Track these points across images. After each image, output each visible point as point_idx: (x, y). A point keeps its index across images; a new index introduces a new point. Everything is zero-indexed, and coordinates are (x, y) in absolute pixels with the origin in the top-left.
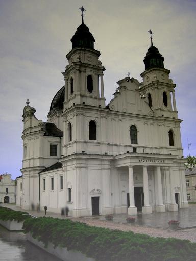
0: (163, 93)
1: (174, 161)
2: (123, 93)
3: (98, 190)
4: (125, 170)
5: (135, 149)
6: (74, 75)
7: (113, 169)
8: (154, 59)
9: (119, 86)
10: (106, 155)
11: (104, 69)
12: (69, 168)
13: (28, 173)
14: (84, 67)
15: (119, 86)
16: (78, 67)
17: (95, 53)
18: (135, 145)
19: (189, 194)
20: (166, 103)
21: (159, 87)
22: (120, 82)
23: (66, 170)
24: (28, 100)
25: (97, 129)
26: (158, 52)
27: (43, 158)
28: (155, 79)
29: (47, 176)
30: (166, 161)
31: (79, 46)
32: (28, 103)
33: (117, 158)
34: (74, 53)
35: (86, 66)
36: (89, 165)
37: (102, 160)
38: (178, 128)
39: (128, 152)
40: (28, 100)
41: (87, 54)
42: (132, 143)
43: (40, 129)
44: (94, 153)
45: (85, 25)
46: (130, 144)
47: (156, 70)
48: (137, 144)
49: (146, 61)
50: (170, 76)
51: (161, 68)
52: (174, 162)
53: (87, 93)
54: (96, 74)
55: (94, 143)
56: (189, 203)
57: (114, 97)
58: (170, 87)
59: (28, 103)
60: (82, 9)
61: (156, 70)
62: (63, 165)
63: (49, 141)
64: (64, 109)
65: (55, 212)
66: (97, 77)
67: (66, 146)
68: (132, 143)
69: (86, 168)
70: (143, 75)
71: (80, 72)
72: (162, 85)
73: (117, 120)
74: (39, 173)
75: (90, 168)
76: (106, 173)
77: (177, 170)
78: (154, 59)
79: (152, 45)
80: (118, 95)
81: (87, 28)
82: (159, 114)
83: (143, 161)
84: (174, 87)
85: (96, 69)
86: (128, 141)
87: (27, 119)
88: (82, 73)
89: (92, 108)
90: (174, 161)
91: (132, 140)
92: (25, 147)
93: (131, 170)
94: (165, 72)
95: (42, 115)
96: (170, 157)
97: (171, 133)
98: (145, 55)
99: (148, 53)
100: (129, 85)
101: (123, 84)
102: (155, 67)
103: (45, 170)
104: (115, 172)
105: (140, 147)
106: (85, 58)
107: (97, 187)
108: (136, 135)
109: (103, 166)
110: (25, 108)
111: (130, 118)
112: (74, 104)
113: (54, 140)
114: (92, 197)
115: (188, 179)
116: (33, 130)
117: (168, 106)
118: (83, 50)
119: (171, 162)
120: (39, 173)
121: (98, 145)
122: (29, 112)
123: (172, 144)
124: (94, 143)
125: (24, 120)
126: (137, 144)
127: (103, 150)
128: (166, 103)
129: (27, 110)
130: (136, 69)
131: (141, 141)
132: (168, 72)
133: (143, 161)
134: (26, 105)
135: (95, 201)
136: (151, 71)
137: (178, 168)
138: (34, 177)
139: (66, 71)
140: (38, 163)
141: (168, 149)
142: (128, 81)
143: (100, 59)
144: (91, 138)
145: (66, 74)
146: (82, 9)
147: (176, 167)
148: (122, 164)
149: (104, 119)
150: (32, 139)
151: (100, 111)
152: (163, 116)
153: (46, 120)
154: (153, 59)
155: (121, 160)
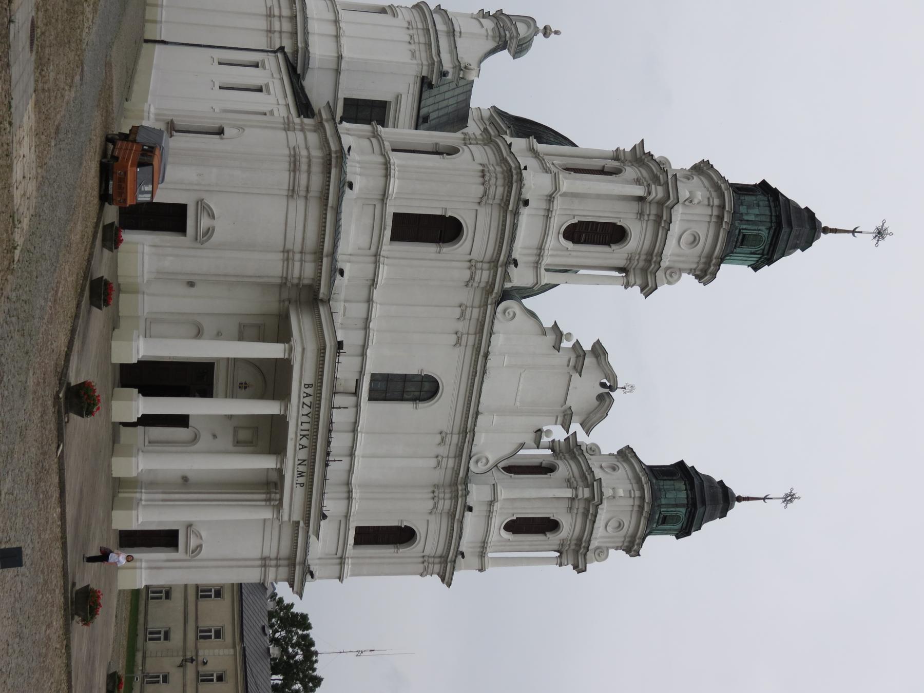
0: (555, 518)
1: (302, 524)
2: (561, 359)
3: (209, 232)
4: (282, 334)
6: (625, 186)
7: (285, 295)
8: (686, 499)
9: (587, 347)
11: (647, 290)
12: (297, 138)
13: (286, 12)
14: (659, 217)
15: (587, 347)
16: (658, 192)
17: (708, 263)
19: (167, 637)
20: (517, 526)
21: (580, 506)
22: (599, 351)
23: (288, 127)
24: (557, 33)
26: (712, 518)
27: (338, 71)
28: (608, 492)
29: (272, 74)
30: (299, 493)
31: (737, 203)
32: (547, 32)
33: (323, 310)
34: (718, 188)
35: (662, 222)
36: (301, 203)
37: (319, 254)
39: (340, 345)
40: (557, 33)
41: (705, 233)
42: (373, 375)
43: (447, 66)
44: (343, 222)
46: (370, 369)
47: (642, 498)
48: (371, 398)
49: (681, 472)
50: (618, 557)
51: (649, 520)
52: (298, 523)
53: (561, 220)
54: (630, 259)
55: (382, 228)
56: (136, 593)
57: (548, 324)
58: (576, 552)
59: (547, 32)
60: (880, 233)
61: (642, 498)
62: (307, 121)
63: (398, 98)
64: (509, 139)
65: (136, 87)
66: (622, 263)
67: (376, 135)
68: (373, 375)
69: (292, 192)
70: (627, 454)
71: (641, 199)
73: (461, 326)
74: (282, 49)
75: (292, 204)
76: (271, 266)
77: (266, 553)
78: (686, 499)
79: (740, 499)
80: (551, 338)
81: (806, 244)
82: (477, 494)
83: (307, 401)
84: (576, 567)
85: (649, 261)
86: (381, 360)
87: (489, 24)
88: (635, 206)
89: (506, 234)
90: (302, 524)
91: (388, 379)
92: (383, 11)
93: (273, 350)
94: (634, 537)
95: (499, 85)
96: (312, 515)
97: (401, 536)
98: (701, 470)
99: (709, 479)
100: (585, 388)
101: (589, 361)
102: (655, 497)
103: (295, 70)
104: (271, 304)
105: (357, 406)
106: (692, 223)
107: (223, 229)
108: (402, 399)
109: (298, 256)
110: (529, 21)
113: (406, 110)
114: (183, 208)
115: (227, 595)
116: (444, 43)
117: (506, 535)
118: (720, 218)
119: (296, 516)
120: (282, 49)
121: (373, 248)
122: (510, 35)
123: (368, 536)
124: (382, 228)
125: (484, 15)
126: (371, 398)
128: (517, 526)
129: (522, 29)
130: (649, 427)
133: (307, 401)
134: (541, 27)
135: (171, 219)
136: (639, 481)
137: (273, 555)
138: (270, 31)
139: (650, 155)
140: (320, 49)
141: (347, 516)
142: (603, 385)
143: (688, 280)
144: (399, 218)
145: (640, 157)
146: (880, 233)
148: (301, 325)
149: (467, 274)
150: (411, 37)
151: (494, 263)
153: (482, 99)
154: (683, 495)
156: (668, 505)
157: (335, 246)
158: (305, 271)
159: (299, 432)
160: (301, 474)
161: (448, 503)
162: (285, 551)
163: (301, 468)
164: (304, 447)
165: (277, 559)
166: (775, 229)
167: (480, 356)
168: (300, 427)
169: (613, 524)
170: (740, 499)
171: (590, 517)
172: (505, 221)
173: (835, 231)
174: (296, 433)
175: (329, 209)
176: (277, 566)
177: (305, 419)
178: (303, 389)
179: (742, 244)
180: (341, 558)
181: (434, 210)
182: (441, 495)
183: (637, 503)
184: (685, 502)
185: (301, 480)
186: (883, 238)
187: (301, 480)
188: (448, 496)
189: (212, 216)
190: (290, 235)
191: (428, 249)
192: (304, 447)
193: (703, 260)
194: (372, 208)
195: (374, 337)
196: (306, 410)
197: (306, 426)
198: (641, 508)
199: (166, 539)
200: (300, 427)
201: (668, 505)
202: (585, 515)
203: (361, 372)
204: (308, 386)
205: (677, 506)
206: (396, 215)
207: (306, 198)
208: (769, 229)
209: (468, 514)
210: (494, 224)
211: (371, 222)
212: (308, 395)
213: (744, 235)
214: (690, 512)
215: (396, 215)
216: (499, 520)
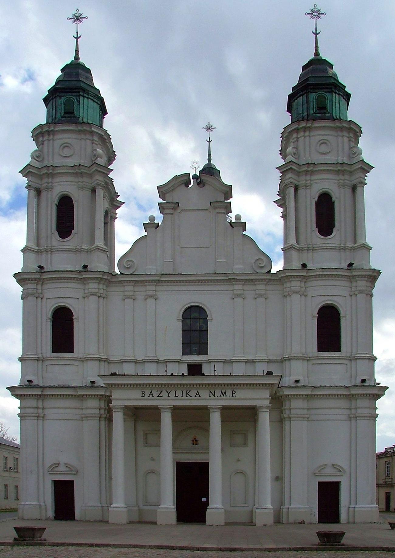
5: (195, 370)
10: (92, 387)
14: (48, 175)
18: (195, 359)
30: (240, 393)
38: (361, 297)
51: (321, 119)
73: (140, 296)
79: (317, 54)
105: (209, 362)
111: (184, 288)
121: (76, 363)
127: (92, 372)
131: (219, 344)
137: (346, 412)
141: (308, 359)
147: (340, 411)
152: (304, 266)
156: (308, 109)
157: (69, 387)
158: (93, 406)
161: (294, 283)
162: (342, 403)
163: (218, 393)
164: (198, 393)
165: (350, 409)
172: (52, 279)
173: (77, 51)
175: (44, 393)
176: (356, 408)
180: (351, 360)
181: (48, 327)
182: (288, 289)
183: (301, 134)
184: (305, 96)
185: (229, 393)
187: (229, 393)
188: (288, 285)
191: (77, 327)
192: (198, 393)
193: (83, 136)
194: (49, 367)
195: (150, 355)
198: (305, 129)
199: (329, 496)
201: (308, 109)
202: (312, 173)
205: (308, 102)
206: (54, 351)
209: (309, 266)
211: (57, 366)
215: (54, 351)
216: (317, 239)
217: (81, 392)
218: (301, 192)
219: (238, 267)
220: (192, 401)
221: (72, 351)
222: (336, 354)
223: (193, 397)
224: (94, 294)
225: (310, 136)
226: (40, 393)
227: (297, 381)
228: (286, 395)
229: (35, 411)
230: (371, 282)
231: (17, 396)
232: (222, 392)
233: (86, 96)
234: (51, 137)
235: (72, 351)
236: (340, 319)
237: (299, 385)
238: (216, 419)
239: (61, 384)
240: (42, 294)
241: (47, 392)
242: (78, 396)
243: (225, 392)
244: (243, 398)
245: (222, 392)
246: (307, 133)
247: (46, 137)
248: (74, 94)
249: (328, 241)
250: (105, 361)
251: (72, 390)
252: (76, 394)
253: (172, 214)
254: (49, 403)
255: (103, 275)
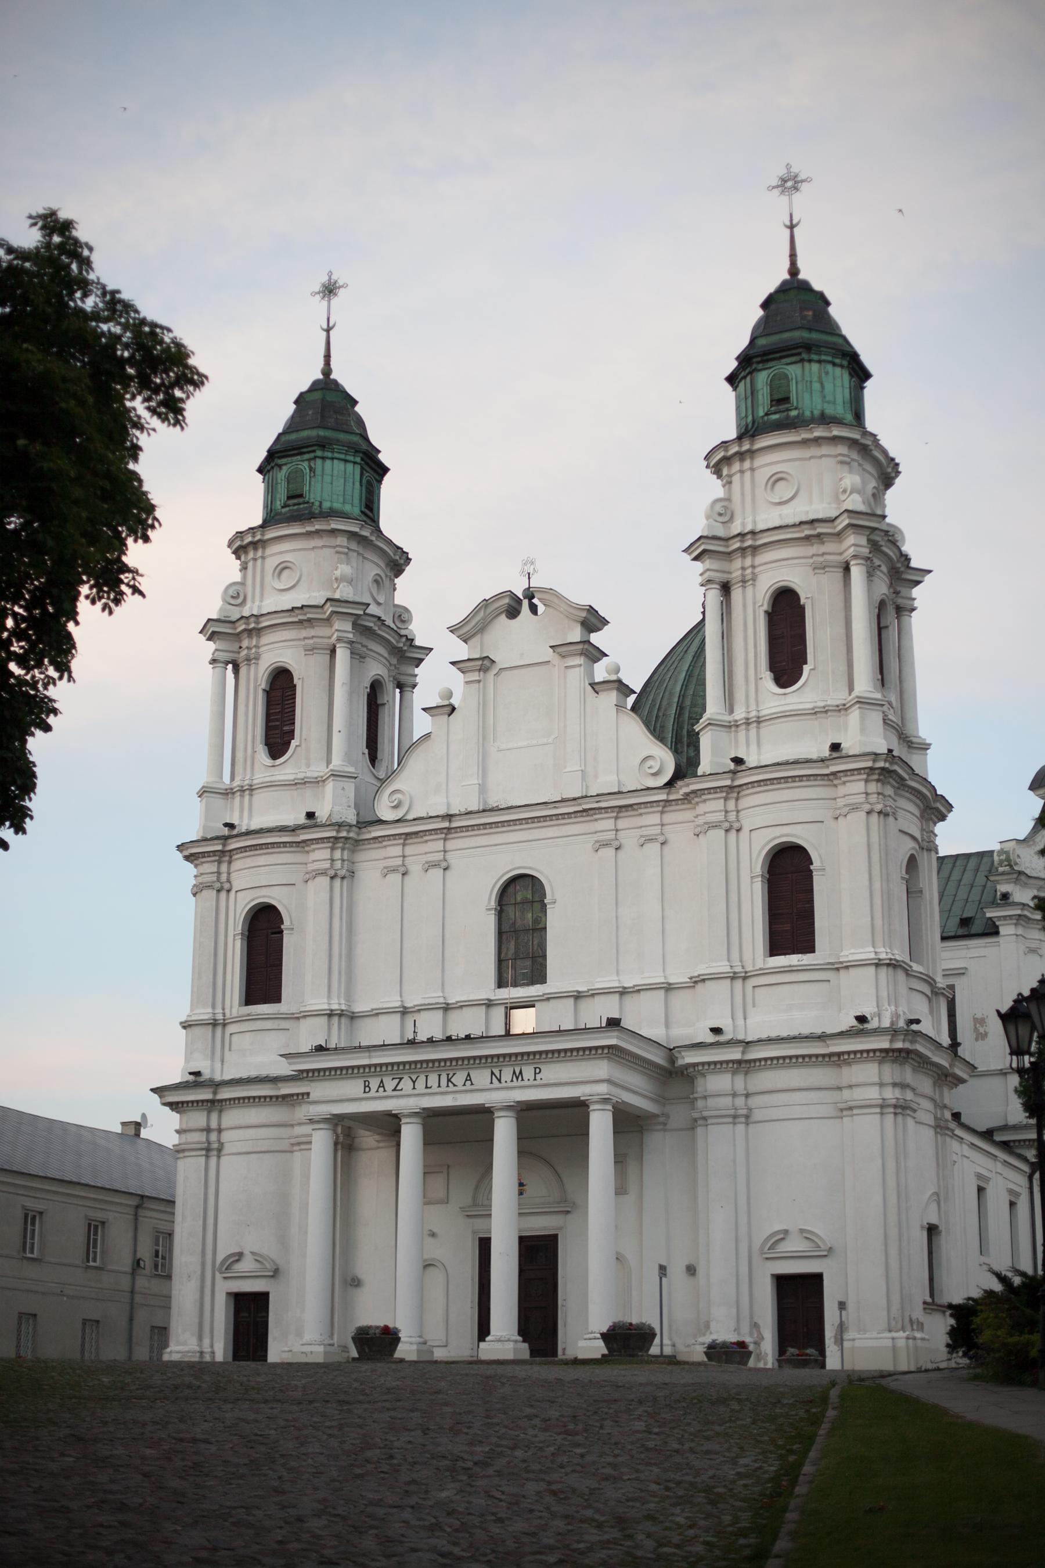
25: (287, 940)
30: (552, 1072)
42: (501, 984)
45: (335, 382)
46: (487, 989)
54: (310, 650)
68: (501, 984)
72: (755, 549)
79: (794, 271)
83: (390, 1084)
107: (256, 1241)
112: (310, 815)
128: (787, 659)
132: (397, 562)
133: (390, 1084)
155: (766, 1068)
159: (444, 1088)
160: (518, 1076)
163: (507, 1074)
164: (469, 1078)
166: (280, 458)
167: (449, 825)
168: (435, 1089)
169: (784, 491)
170: (794, 271)
171: (749, 543)
174: (442, 1093)
177: (421, 1080)
178: (373, 1093)
179: (301, 496)
183: (736, 466)
186: (324, 285)
187: (528, 1072)
189: (239, 1256)
190: (263, 1146)
192: (469, 1078)
196: (406, 1084)
197: (433, 1080)
200: (435, 1089)
203: (489, 1004)
204: (367, 1086)
207: (220, 1131)
208: (280, 466)
209: (751, 761)
210: (250, 862)
212: (382, 1085)
213: (289, 498)
214: (762, 362)
216: (772, 698)
217: (286, 1089)
218: (736, 594)
219: (605, 782)
220: (458, 1096)
221: (277, 999)
222: (805, 959)
223: (460, 1088)
224: (323, 873)
225: (752, 469)
226: (209, 1096)
227: (716, 1031)
228: (695, 1065)
229: (201, 1137)
230: (878, 781)
231: (174, 1106)
232: (514, 1072)
233: (329, 455)
234: (260, 553)
235: (277, 999)
236: (809, 875)
237: (722, 1038)
238: (504, 1133)
239: (253, 1073)
240: (229, 881)
241: (225, 1094)
242: (284, 1097)
243: (521, 1073)
244: (557, 1083)
245: (514, 1072)
246: (747, 464)
247: (251, 555)
248: (306, 456)
249: (790, 699)
250: (340, 1015)
251: (269, 1086)
252: (278, 1093)
253: (479, 681)
254: (232, 1117)
255: (338, 831)
